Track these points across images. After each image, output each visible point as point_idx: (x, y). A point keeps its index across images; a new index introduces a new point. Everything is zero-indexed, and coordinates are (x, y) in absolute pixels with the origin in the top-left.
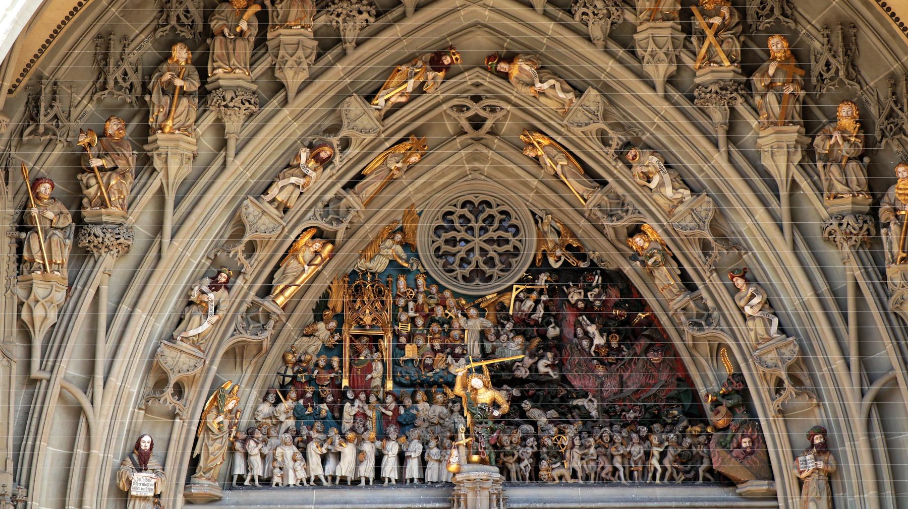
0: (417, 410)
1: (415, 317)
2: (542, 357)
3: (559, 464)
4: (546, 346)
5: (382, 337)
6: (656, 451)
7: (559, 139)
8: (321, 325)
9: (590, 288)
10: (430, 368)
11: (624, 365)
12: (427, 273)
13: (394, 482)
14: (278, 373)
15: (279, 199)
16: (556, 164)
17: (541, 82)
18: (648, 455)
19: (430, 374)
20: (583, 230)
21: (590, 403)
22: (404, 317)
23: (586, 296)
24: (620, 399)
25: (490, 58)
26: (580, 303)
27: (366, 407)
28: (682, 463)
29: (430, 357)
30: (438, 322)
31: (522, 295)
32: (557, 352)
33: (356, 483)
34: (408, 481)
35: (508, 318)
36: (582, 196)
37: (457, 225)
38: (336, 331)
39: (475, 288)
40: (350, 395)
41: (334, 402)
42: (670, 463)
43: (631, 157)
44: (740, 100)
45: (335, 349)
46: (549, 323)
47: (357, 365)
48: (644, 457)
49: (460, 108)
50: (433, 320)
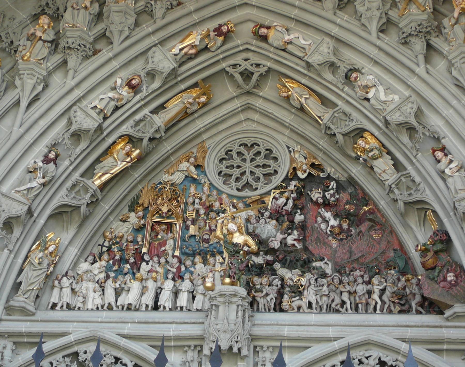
0: (195, 269)
1: (199, 209)
2: (289, 234)
3: (298, 298)
4: (292, 225)
5: (176, 224)
6: (377, 289)
7: (304, 81)
8: (132, 215)
9: (327, 190)
10: (207, 241)
11: (352, 238)
12: (211, 184)
13: (167, 309)
14: (99, 245)
15: (99, 107)
16: (301, 96)
17: (289, 35)
18: (370, 293)
19: (207, 245)
20: (325, 153)
21: (325, 264)
22: (190, 208)
23: (324, 196)
24: (349, 262)
25: (254, 27)
26: (319, 199)
27: (157, 265)
28: (399, 299)
29: (207, 234)
30: (215, 211)
31: (277, 196)
32: (302, 232)
33: (137, 310)
34: (179, 308)
35: (266, 210)
36: (319, 117)
37: (235, 155)
38: (142, 219)
39: (246, 193)
40: (146, 258)
41: (135, 263)
42: (388, 297)
43: (353, 79)
44: (434, 34)
45: (140, 229)
46: (295, 213)
47: (156, 241)
48: (367, 296)
49: (234, 66)
50: (212, 211)
